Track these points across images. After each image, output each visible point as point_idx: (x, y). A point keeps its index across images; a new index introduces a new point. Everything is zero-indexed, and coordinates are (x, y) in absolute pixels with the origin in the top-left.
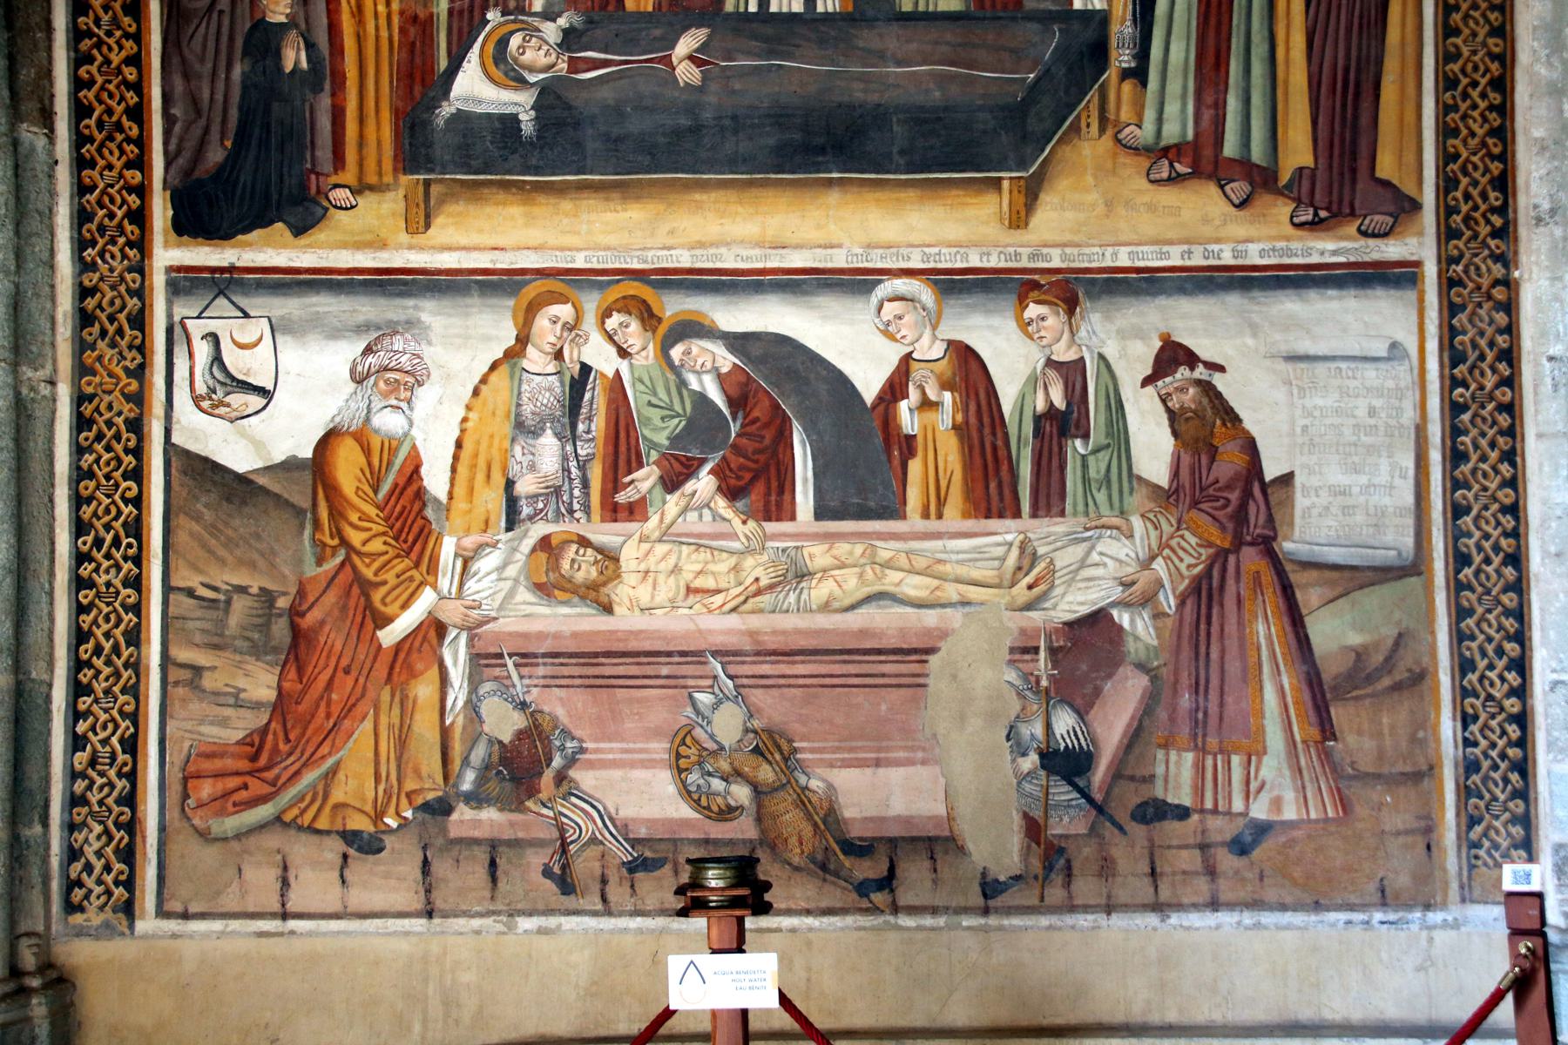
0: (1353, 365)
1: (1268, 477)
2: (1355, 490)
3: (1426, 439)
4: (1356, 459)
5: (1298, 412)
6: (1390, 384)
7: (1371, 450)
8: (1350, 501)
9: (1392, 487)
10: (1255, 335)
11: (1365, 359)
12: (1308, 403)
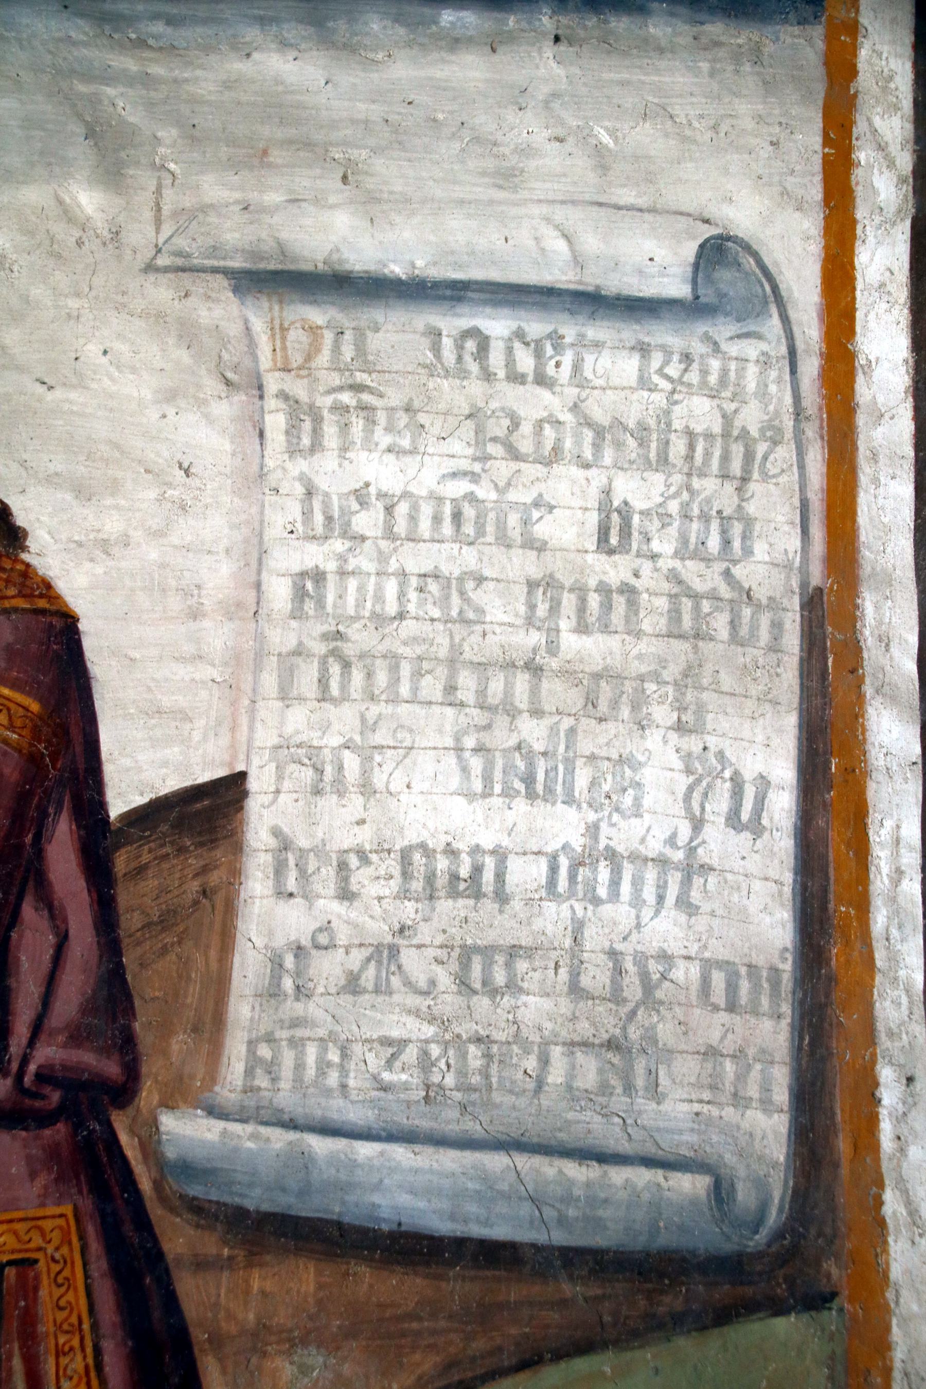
0: (537, 326)
1: (122, 797)
2: (525, 874)
3: (852, 652)
4: (533, 732)
5: (284, 513)
6: (700, 412)
7: (602, 693)
8: (497, 926)
9: (693, 869)
10: (112, 174)
11: (592, 302)
12: (331, 473)
